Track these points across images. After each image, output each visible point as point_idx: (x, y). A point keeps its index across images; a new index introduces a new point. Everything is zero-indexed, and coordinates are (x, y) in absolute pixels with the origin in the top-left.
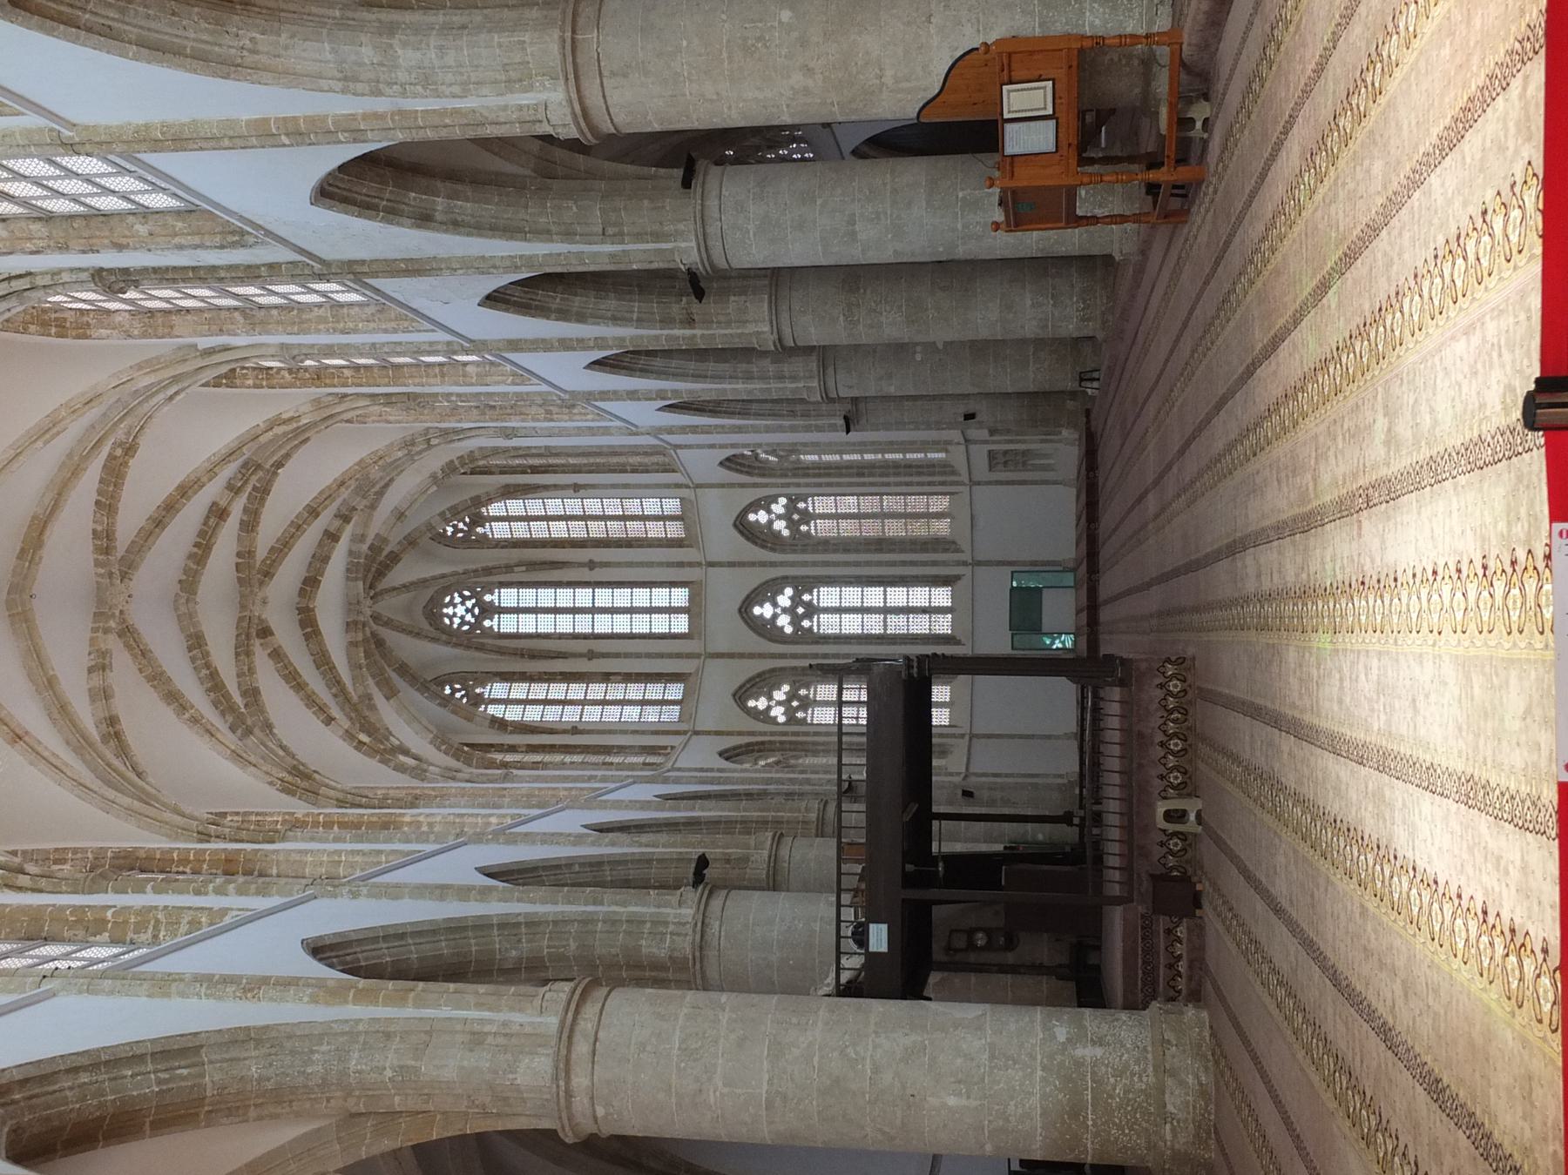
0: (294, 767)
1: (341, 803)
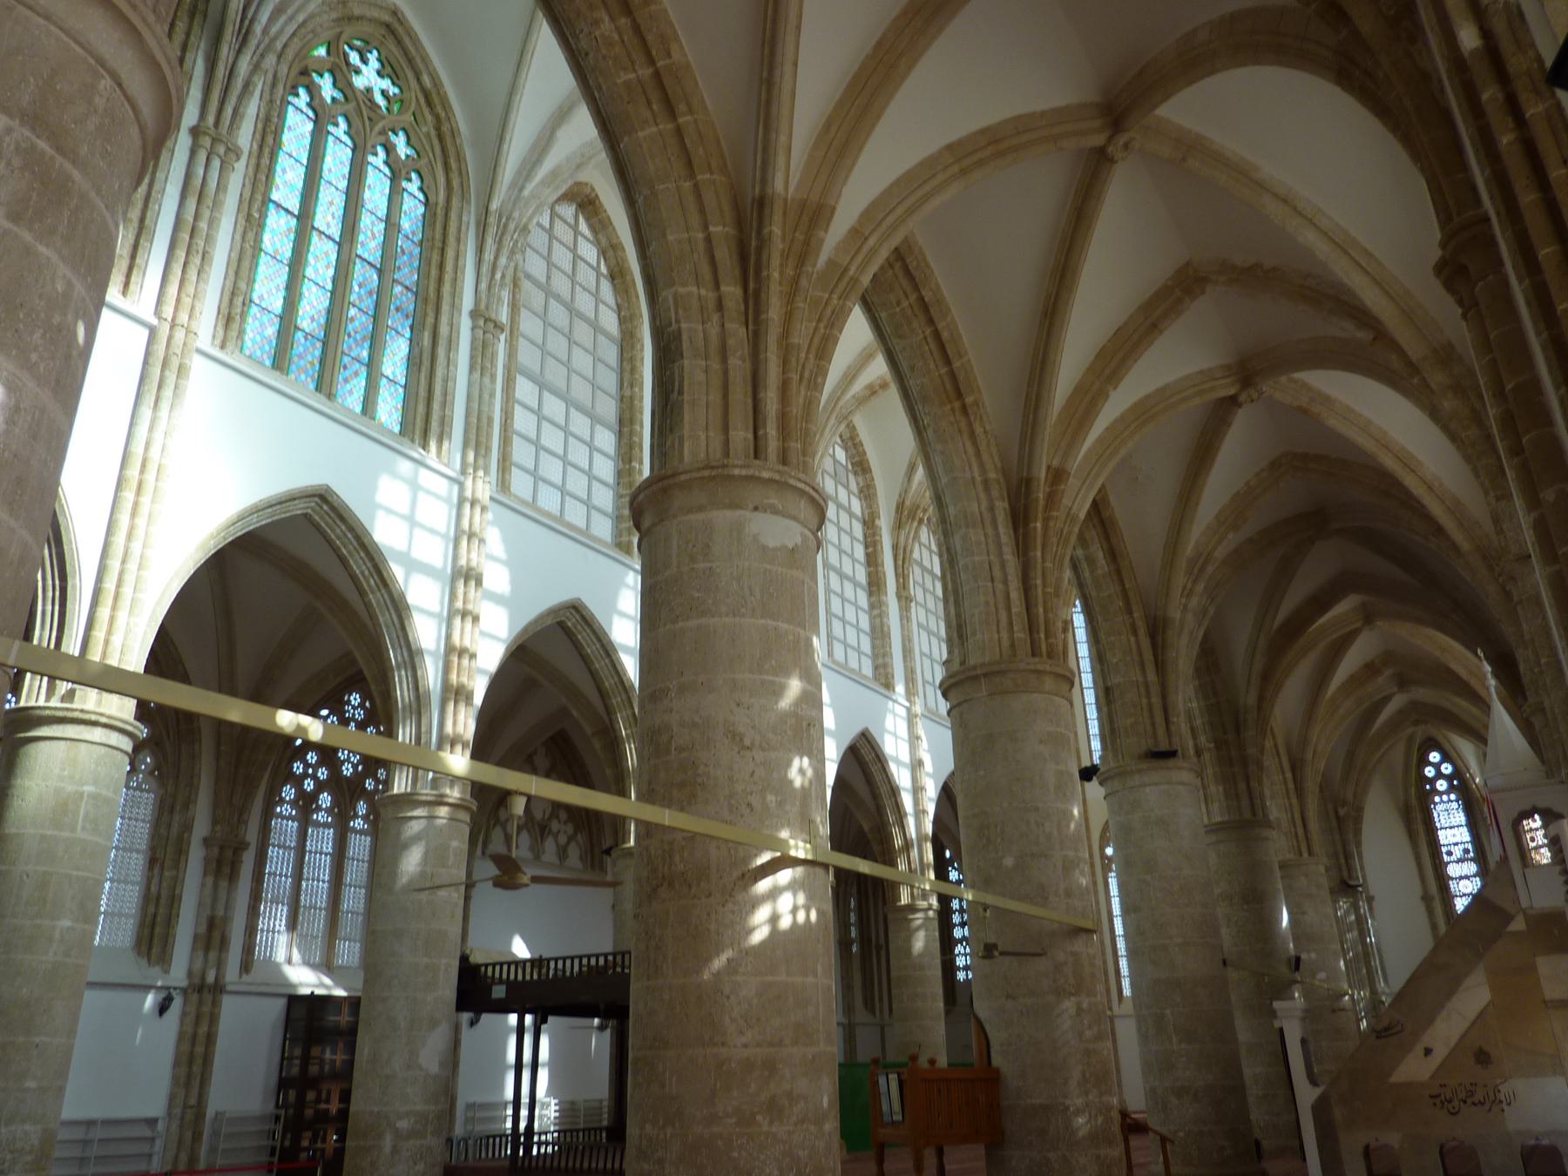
0: (918, 507)
1: (895, 548)
